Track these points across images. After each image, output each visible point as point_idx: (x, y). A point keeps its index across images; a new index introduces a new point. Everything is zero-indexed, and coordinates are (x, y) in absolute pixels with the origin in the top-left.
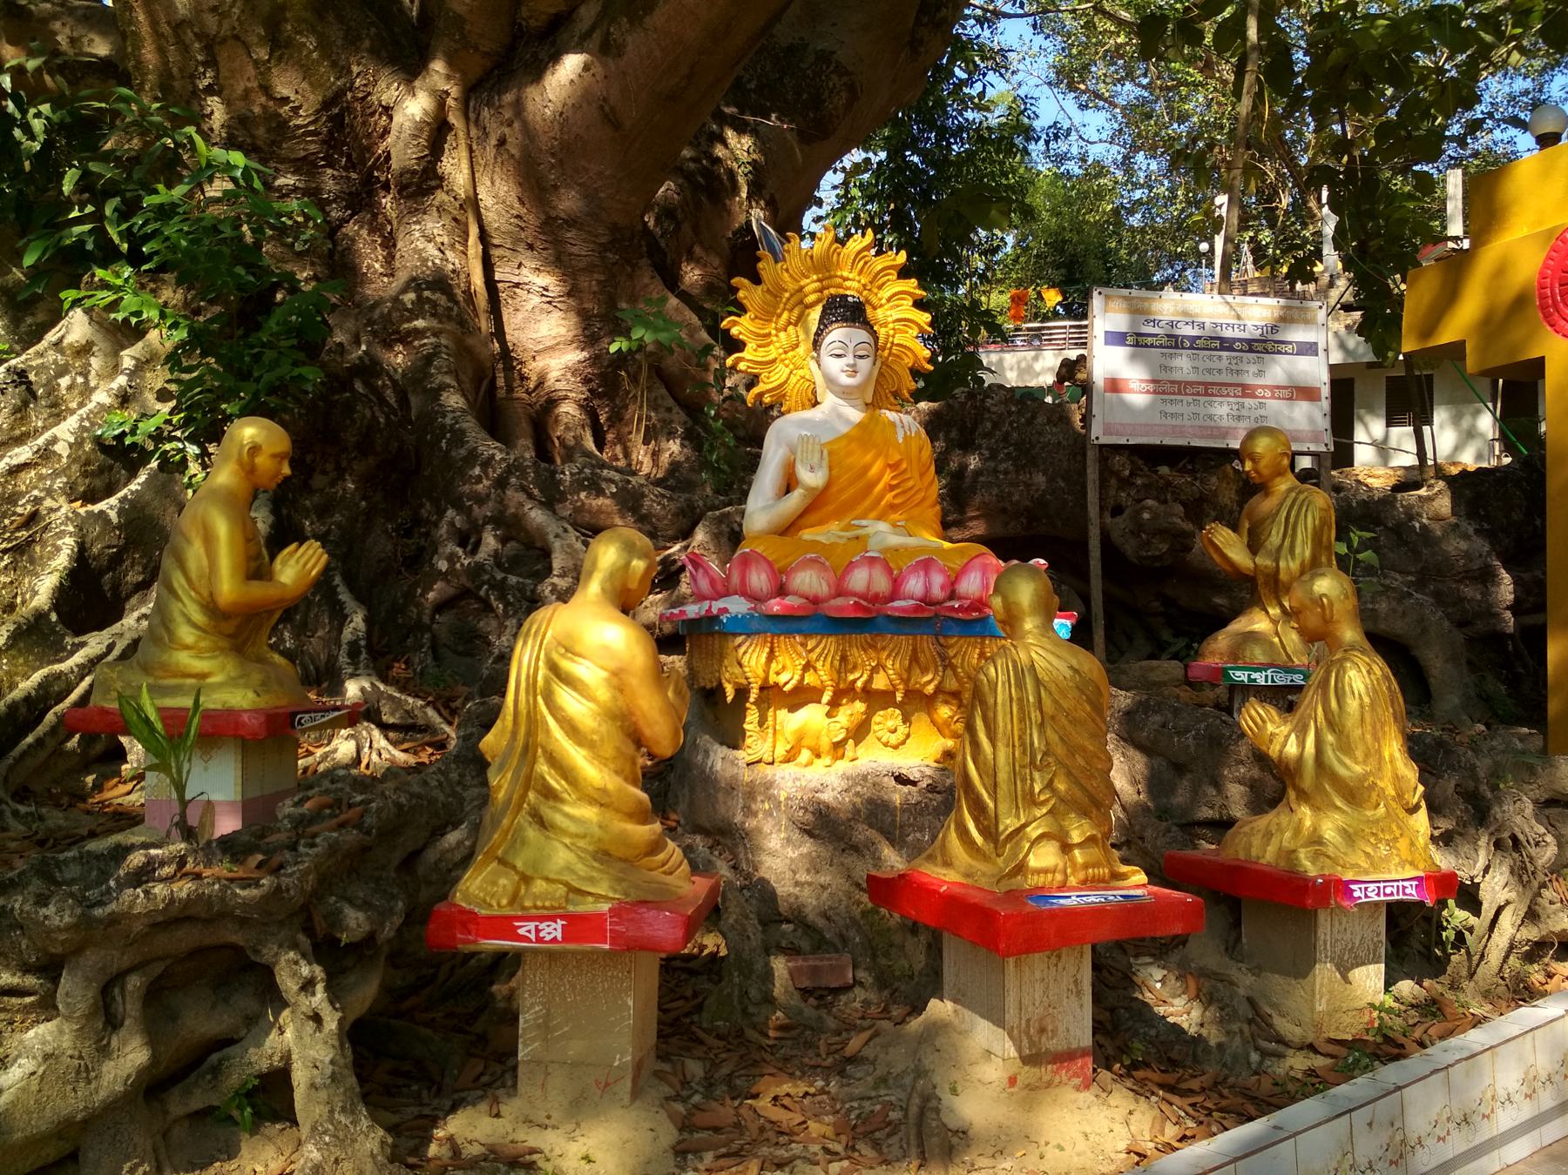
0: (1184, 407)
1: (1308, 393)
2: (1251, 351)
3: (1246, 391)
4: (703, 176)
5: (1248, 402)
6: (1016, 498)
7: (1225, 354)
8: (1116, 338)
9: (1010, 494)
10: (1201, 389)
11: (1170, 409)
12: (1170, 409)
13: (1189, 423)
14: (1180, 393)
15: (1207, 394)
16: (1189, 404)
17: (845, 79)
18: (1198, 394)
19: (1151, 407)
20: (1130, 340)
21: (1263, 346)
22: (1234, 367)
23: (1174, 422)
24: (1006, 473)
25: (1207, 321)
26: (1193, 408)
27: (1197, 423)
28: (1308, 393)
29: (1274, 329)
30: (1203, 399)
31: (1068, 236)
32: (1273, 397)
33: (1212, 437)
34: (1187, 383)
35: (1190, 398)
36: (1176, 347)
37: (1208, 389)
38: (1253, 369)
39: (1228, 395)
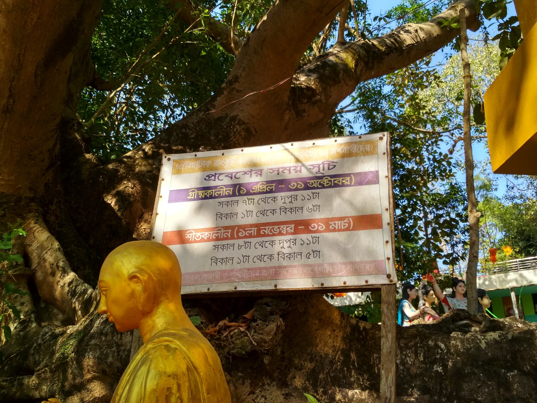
0: (236, 250)
1: (368, 221)
2: (307, 188)
3: (303, 226)
4: (150, 179)
5: (304, 237)
6: (110, 359)
7: (279, 195)
8: (178, 196)
9: (107, 355)
10: (254, 231)
11: (222, 254)
12: (222, 254)
13: (239, 267)
14: (232, 238)
15: (259, 235)
16: (240, 247)
17: (243, 126)
18: (251, 236)
19: (204, 256)
20: (191, 195)
21: (328, 180)
22: (288, 206)
23: (223, 267)
24: (106, 335)
25: (265, 168)
26: (244, 251)
27: (247, 265)
28: (368, 221)
29: (332, 165)
30: (254, 240)
31: (524, 228)
32: (328, 230)
33: (261, 279)
34: (240, 227)
35: (241, 242)
36: (234, 195)
37: (261, 230)
38: (309, 205)
39: (280, 234)
